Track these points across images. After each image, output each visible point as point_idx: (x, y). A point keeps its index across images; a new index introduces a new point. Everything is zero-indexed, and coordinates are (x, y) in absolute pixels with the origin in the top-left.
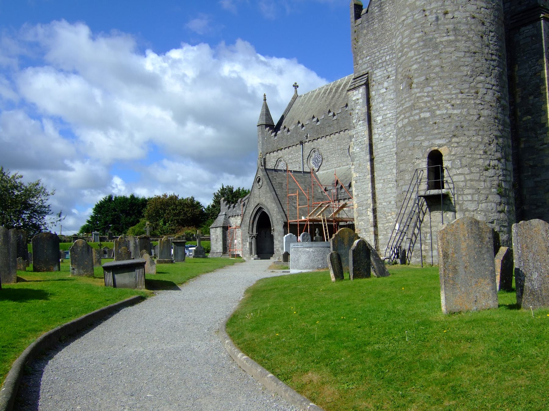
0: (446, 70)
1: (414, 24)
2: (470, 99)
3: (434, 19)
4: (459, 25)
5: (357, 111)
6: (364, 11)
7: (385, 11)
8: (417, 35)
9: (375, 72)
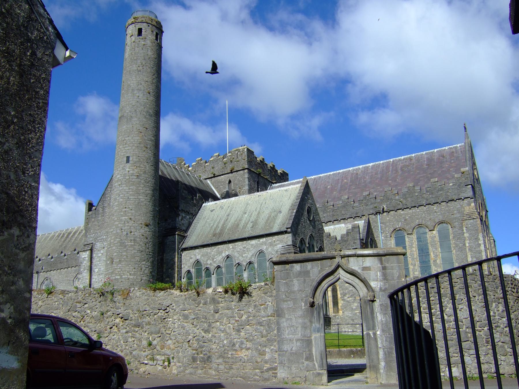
0: (129, 257)
1: (117, 234)
2: (138, 272)
3: (126, 234)
4: (136, 238)
5: (84, 264)
6: (94, 208)
7: (106, 212)
8: (118, 240)
9: (97, 244)
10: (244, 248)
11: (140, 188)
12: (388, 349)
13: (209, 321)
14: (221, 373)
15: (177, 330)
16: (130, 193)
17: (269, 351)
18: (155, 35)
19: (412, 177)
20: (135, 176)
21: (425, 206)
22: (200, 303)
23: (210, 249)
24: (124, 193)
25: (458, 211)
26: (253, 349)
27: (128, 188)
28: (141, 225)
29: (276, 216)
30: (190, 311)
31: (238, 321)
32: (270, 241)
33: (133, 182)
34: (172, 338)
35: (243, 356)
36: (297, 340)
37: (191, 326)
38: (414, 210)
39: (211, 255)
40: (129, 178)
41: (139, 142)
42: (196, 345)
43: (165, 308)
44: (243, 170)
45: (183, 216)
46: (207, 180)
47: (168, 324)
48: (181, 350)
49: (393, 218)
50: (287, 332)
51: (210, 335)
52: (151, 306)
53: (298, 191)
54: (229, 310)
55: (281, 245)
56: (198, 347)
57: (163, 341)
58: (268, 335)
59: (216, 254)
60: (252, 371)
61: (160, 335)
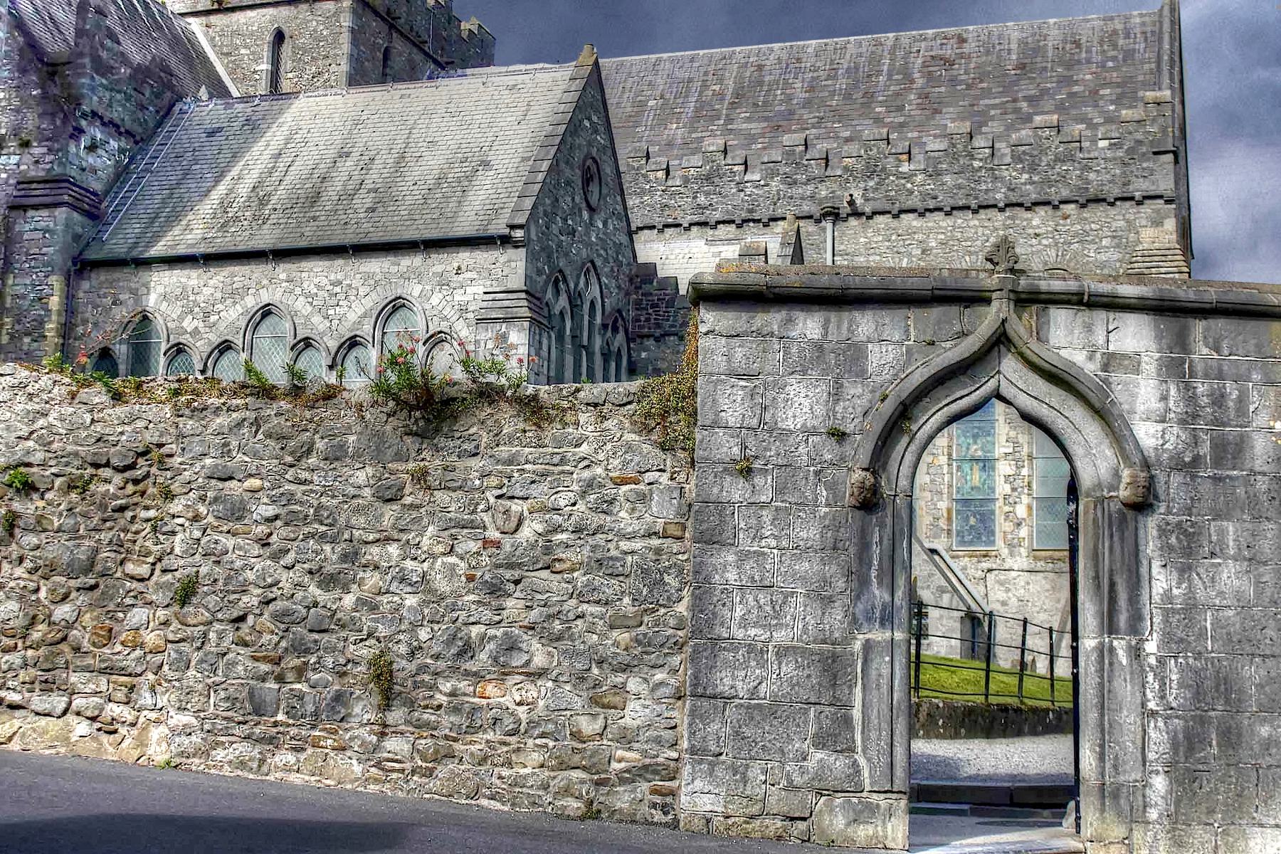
12: (1186, 721)
13: (346, 536)
14: (393, 771)
15: (182, 562)
17: (643, 689)
19: (961, 103)
21: (1001, 210)
22: (309, 452)
23: (198, 277)
25: (1116, 241)
26: (561, 679)
29: (470, 179)
30: (255, 483)
31: (497, 545)
32: (439, 268)
34: (154, 597)
35: (512, 706)
36: (783, 652)
37: (256, 553)
38: (960, 219)
39: (200, 298)
42: (276, 638)
43: (129, 461)
47: (137, 533)
48: (196, 657)
49: (881, 238)
50: (739, 612)
51: (349, 600)
52: (55, 446)
53: (558, 92)
54: (453, 495)
55: (481, 290)
56: (286, 649)
57: (111, 607)
58: (646, 619)
59: (219, 295)
60: (552, 774)
61: (92, 582)
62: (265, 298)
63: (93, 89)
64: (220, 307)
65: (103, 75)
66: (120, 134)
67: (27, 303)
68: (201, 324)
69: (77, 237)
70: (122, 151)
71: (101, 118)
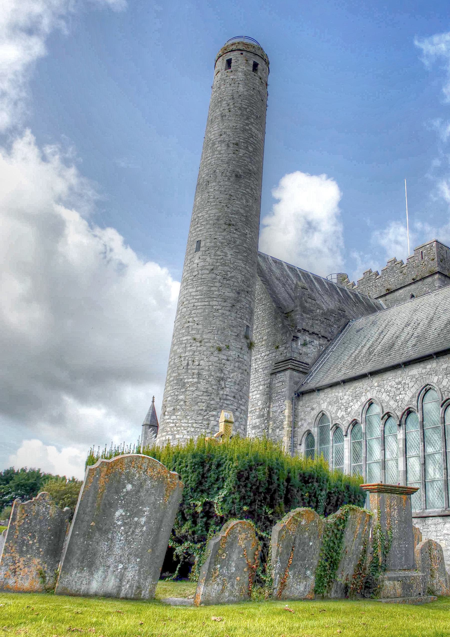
1: (173, 366)
2: (202, 428)
3: (186, 364)
4: (202, 371)
8: (174, 375)
10: (400, 383)
11: (213, 289)
16: (198, 297)
18: (252, 66)
20: (207, 269)
23: (342, 392)
24: (189, 298)
27: (194, 290)
28: (212, 349)
33: (203, 280)
40: (198, 274)
41: (216, 217)
44: (432, 274)
45: (305, 340)
46: (379, 300)
62: (369, 396)
63: (303, 319)
64: (351, 404)
65: (307, 314)
66: (320, 338)
67: (278, 414)
68: (344, 413)
69: (296, 383)
70: (320, 345)
71: (308, 331)
